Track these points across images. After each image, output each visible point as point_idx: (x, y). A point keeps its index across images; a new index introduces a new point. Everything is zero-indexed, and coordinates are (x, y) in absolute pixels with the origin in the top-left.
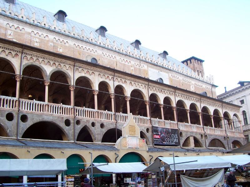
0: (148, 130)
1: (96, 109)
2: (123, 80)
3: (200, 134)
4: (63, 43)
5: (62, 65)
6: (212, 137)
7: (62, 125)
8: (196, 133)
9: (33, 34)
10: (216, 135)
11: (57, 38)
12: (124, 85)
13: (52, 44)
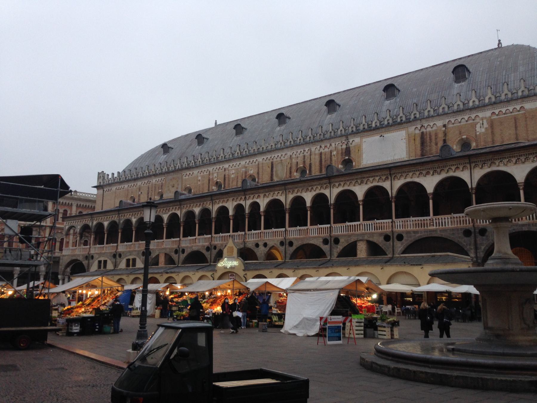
0: (282, 243)
1: (231, 233)
2: (256, 196)
3: (381, 234)
4: (254, 164)
5: (205, 203)
6: (418, 235)
7: (204, 252)
8: (372, 234)
9: (230, 168)
10: (435, 231)
11: (248, 161)
12: (258, 201)
13: (244, 169)
